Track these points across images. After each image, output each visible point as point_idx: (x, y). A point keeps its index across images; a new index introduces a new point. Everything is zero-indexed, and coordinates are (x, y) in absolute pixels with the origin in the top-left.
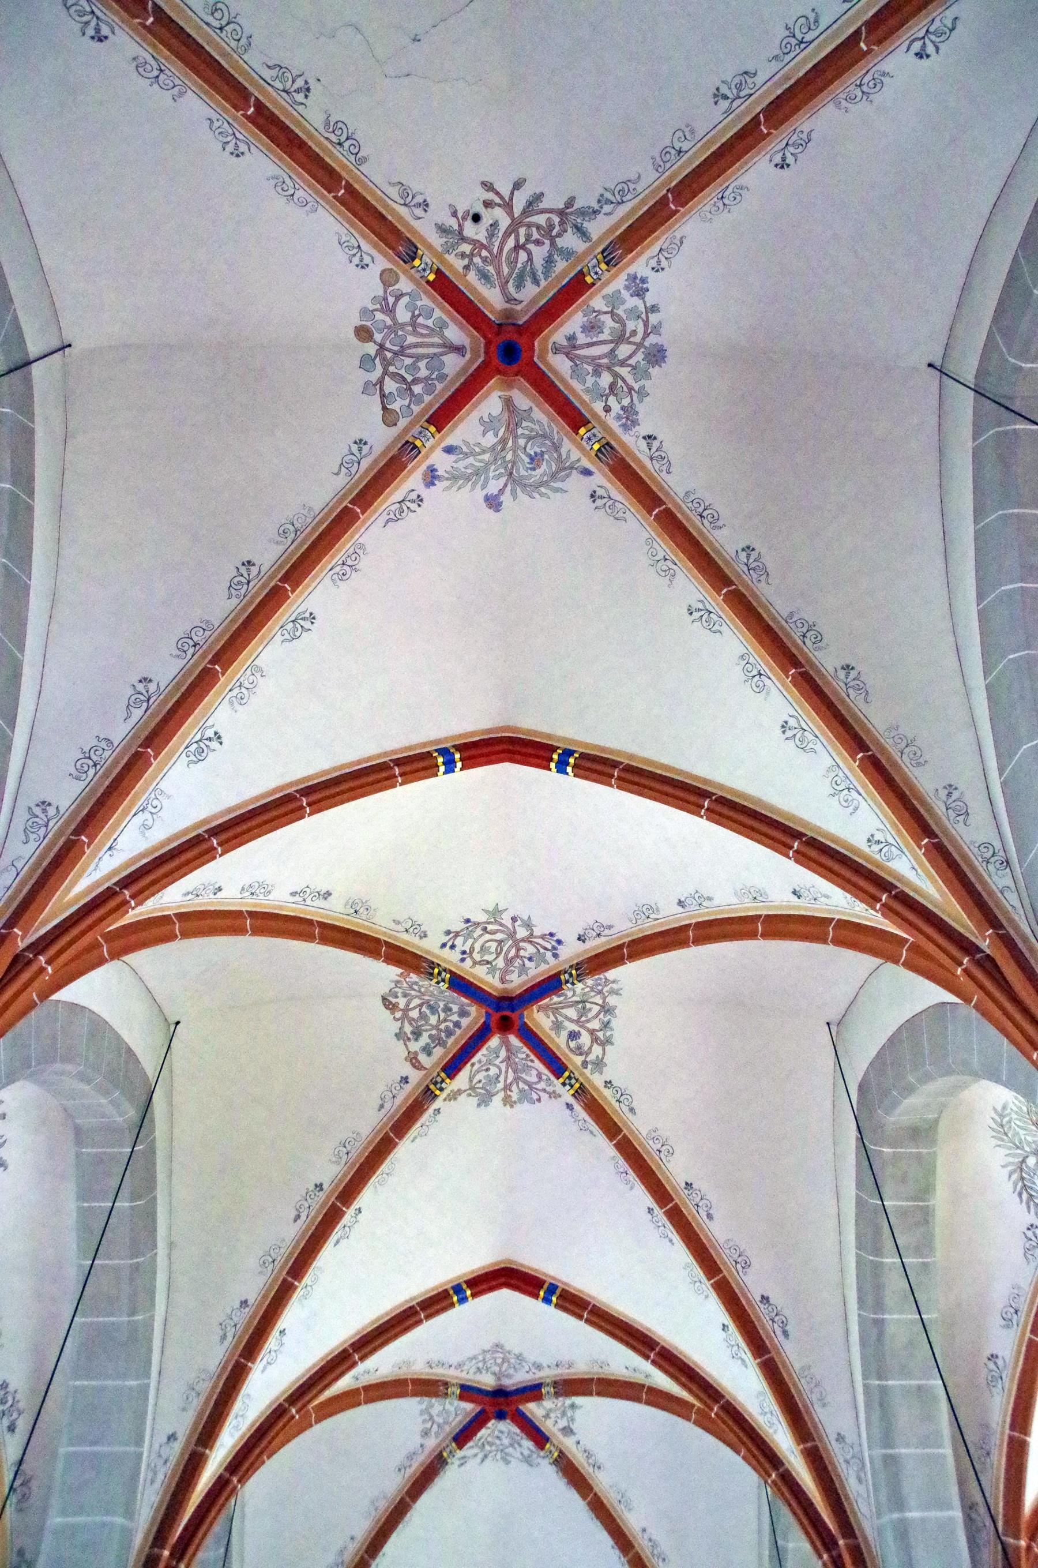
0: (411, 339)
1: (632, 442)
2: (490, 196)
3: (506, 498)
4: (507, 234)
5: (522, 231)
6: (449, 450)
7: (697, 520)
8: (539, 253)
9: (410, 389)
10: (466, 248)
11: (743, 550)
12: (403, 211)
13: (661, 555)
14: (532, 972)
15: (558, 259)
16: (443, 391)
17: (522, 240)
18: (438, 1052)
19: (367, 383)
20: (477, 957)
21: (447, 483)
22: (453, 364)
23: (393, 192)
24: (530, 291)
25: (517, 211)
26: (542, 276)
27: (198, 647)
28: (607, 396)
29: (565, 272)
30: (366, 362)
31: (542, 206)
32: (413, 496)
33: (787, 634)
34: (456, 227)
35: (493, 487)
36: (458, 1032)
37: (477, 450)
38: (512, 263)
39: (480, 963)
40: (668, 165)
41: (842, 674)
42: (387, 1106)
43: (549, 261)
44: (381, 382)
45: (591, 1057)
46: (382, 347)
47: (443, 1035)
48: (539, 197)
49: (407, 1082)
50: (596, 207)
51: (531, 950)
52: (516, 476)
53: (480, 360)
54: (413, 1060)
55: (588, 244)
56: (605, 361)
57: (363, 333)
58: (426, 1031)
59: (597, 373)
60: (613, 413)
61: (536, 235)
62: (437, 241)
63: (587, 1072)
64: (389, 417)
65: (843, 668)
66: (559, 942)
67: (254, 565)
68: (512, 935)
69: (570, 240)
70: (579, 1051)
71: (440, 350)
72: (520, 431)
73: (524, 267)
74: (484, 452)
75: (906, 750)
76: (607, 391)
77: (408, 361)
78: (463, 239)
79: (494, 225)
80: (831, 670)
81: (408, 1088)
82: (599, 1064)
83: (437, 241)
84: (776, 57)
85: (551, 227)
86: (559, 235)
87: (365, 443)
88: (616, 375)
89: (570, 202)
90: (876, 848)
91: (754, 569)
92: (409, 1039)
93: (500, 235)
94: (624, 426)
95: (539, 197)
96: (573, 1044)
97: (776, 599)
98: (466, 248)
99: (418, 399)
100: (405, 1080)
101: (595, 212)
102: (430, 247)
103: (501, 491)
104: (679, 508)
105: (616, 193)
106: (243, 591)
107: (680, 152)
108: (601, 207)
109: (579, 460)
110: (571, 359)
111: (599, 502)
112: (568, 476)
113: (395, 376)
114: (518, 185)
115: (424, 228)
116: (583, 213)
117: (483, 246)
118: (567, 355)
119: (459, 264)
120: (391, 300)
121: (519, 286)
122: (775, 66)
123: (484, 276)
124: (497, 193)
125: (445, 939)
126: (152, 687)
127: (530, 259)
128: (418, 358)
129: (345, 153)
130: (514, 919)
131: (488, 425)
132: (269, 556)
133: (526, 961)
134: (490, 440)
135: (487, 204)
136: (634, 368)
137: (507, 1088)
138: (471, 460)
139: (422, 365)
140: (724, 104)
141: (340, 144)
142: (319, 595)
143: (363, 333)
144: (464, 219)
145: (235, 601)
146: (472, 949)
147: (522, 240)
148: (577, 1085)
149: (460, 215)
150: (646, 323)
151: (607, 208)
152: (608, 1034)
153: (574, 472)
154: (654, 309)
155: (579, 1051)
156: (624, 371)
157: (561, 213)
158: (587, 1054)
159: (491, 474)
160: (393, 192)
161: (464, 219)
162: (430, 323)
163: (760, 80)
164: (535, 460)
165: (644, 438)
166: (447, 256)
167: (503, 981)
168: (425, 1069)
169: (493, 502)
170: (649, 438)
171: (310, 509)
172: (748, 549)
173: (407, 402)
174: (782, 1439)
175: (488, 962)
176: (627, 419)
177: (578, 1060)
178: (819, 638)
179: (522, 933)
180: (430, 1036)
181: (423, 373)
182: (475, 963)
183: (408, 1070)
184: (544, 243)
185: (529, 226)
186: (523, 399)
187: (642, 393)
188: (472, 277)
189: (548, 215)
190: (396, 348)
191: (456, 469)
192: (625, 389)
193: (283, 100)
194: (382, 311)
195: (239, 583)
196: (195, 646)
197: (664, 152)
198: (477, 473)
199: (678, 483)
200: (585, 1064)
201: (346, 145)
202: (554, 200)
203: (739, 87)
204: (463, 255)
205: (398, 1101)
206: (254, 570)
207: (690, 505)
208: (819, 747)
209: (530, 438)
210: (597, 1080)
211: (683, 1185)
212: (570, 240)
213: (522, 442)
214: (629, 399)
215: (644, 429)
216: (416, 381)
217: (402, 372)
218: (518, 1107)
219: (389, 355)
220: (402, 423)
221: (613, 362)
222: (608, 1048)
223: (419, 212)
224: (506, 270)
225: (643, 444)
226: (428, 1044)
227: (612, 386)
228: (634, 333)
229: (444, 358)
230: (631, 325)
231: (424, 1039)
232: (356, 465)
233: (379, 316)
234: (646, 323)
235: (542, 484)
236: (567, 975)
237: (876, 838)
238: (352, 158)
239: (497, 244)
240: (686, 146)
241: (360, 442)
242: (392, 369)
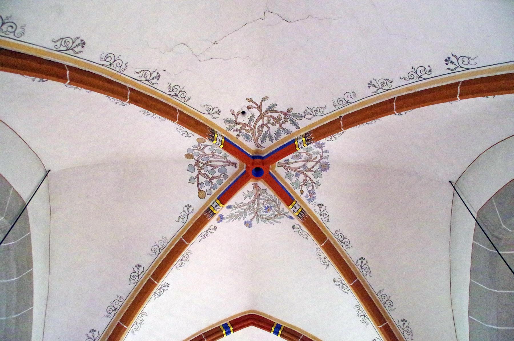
0: (211, 159)
1: (313, 207)
2: (251, 104)
3: (254, 222)
4: (257, 121)
5: (266, 119)
6: (229, 207)
7: (339, 244)
8: (274, 129)
9: (211, 181)
10: (238, 127)
11: (360, 259)
12: (208, 117)
13: (323, 256)
15: (283, 133)
16: (226, 183)
17: (265, 122)
19: (191, 178)
21: (227, 220)
22: (231, 171)
23: (203, 110)
24: (268, 144)
25: (264, 110)
26: (274, 138)
27: (116, 311)
28: (302, 186)
29: (286, 139)
30: (190, 168)
31: (275, 109)
32: (213, 227)
33: (378, 302)
34: (234, 119)
35: (248, 218)
37: (241, 205)
38: (260, 132)
40: (341, 106)
41: (401, 323)
43: (278, 133)
44: (197, 177)
46: (198, 161)
48: (275, 105)
50: (303, 115)
52: (258, 213)
53: (244, 170)
55: (297, 130)
56: (302, 169)
57: (189, 156)
59: (297, 175)
60: (304, 194)
61: (272, 121)
62: (224, 126)
64: (201, 194)
65: (402, 321)
67: (141, 266)
69: (288, 126)
71: (225, 164)
72: (261, 197)
73: (266, 134)
74: (244, 205)
76: (302, 183)
77: (210, 168)
78: (237, 123)
79: (253, 116)
80: (397, 322)
83: (224, 126)
84: (404, 78)
85: (280, 119)
86: (283, 123)
87: (191, 207)
88: (306, 176)
89: (290, 110)
91: (364, 269)
93: (255, 119)
94: (309, 200)
95: (275, 105)
97: (375, 283)
98: (238, 127)
99: (214, 186)
101: (302, 117)
102: (221, 129)
103: (252, 220)
104: (333, 239)
105: (313, 110)
106: (136, 280)
107: (348, 102)
108: (305, 115)
109: (288, 212)
110: (286, 169)
111: (296, 230)
112: (283, 217)
113: (204, 175)
114: (264, 99)
115: (219, 123)
116: (295, 115)
117: (246, 125)
118: (284, 167)
119: (235, 134)
120: (202, 147)
121: (263, 141)
122: (403, 82)
123: (247, 137)
124: (255, 103)
126: (96, 334)
127: (269, 130)
128: (215, 167)
129: (178, 99)
131: (245, 196)
132: (148, 261)
134: (248, 200)
135: (249, 108)
136: (315, 172)
138: (239, 209)
139: (217, 170)
140: (373, 89)
141: (176, 95)
142: (172, 276)
143: (189, 156)
144: (238, 115)
145: (132, 286)
147: (265, 122)
149: (235, 114)
150: (322, 155)
151: (308, 116)
153: (285, 216)
154: (326, 151)
156: (310, 174)
157: (285, 114)
159: (248, 214)
160: (203, 110)
161: (238, 115)
162: (221, 155)
163: (394, 85)
164: (267, 209)
165: (318, 205)
166: (229, 132)
169: (248, 224)
170: (320, 205)
171: (166, 238)
172: (362, 259)
173: (209, 188)
176: (311, 196)
178: (391, 305)
181: (217, 174)
184: (276, 125)
185: (269, 117)
186: (262, 185)
187: (318, 184)
188: (241, 138)
189: (277, 114)
190: (204, 162)
191: (232, 214)
192: (310, 182)
193: (146, 85)
194: (197, 149)
195: (134, 276)
196: (115, 310)
197: (340, 100)
198: (241, 214)
199: (332, 227)
201: (179, 95)
202: (282, 107)
203: (383, 84)
204: (237, 130)
206: (141, 269)
207: (337, 237)
209: (266, 200)
212: (288, 126)
213: (262, 201)
214: (311, 187)
215: (318, 201)
216: (214, 178)
217: (207, 173)
219: (201, 165)
220: (208, 197)
221: (304, 170)
223: (216, 115)
224: (257, 134)
225: (317, 208)
227: (304, 181)
228: (316, 158)
229: (227, 167)
230: (314, 156)
232: (186, 217)
233: (196, 151)
234: (322, 155)
235: (270, 218)
238: (182, 100)
239: (253, 124)
240: (351, 100)
241: (188, 206)
242: (202, 171)
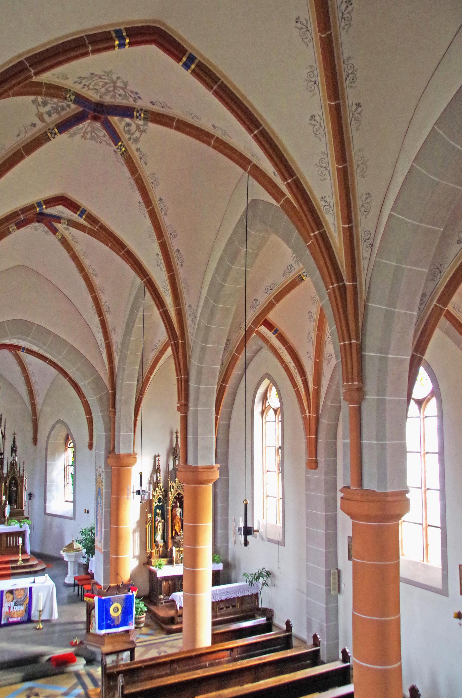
14: (117, 100)
18: (55, 116)
20: (91, 87)
36: (68, 109)
39: (91, 89)
42: (22, 135)
45: (134, 136)
47: (59, 109)
49: (35, 126)
51: (121, 92)
54: (40, 116)
58: (51, 104)
63: (130, 143)
66: (140, 98)
68: (114, 83)
70: (129, 132)
75: (361, 166)
81: (35, 130)
82: (136, 140)
90: (323, 203)
92: (39, 105)
96: (126, 129)
100: (34, 125)
125: (77, 80)
130: (118, 78)
133: (117, 96)
137: (86, 132)
146: (90, 84)
148: (124, 149)
152: (146, 128)
155: (129, 132)
158: (132, 134)
167: (101, 97)
168: (46, 123)
174: (168, 300)
175: (96, 89)
177: (127, 136)
179: (119, 84)
180: (52, 107)
182: (89, 89)
183: (36, 120)
200: (130, 139)
205: (29, 134)
208: (323, 140)
210: (134, 147)
211: (158, 199)
218: (88, 142)
222: (143, 134)
226: (50, 111)
231: (48, 108)
236: (138, 114)
237: (326, 199)
